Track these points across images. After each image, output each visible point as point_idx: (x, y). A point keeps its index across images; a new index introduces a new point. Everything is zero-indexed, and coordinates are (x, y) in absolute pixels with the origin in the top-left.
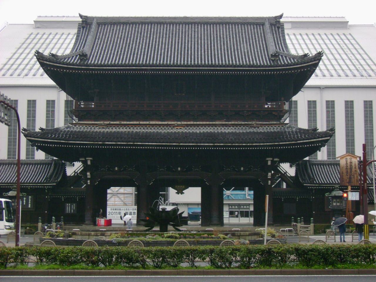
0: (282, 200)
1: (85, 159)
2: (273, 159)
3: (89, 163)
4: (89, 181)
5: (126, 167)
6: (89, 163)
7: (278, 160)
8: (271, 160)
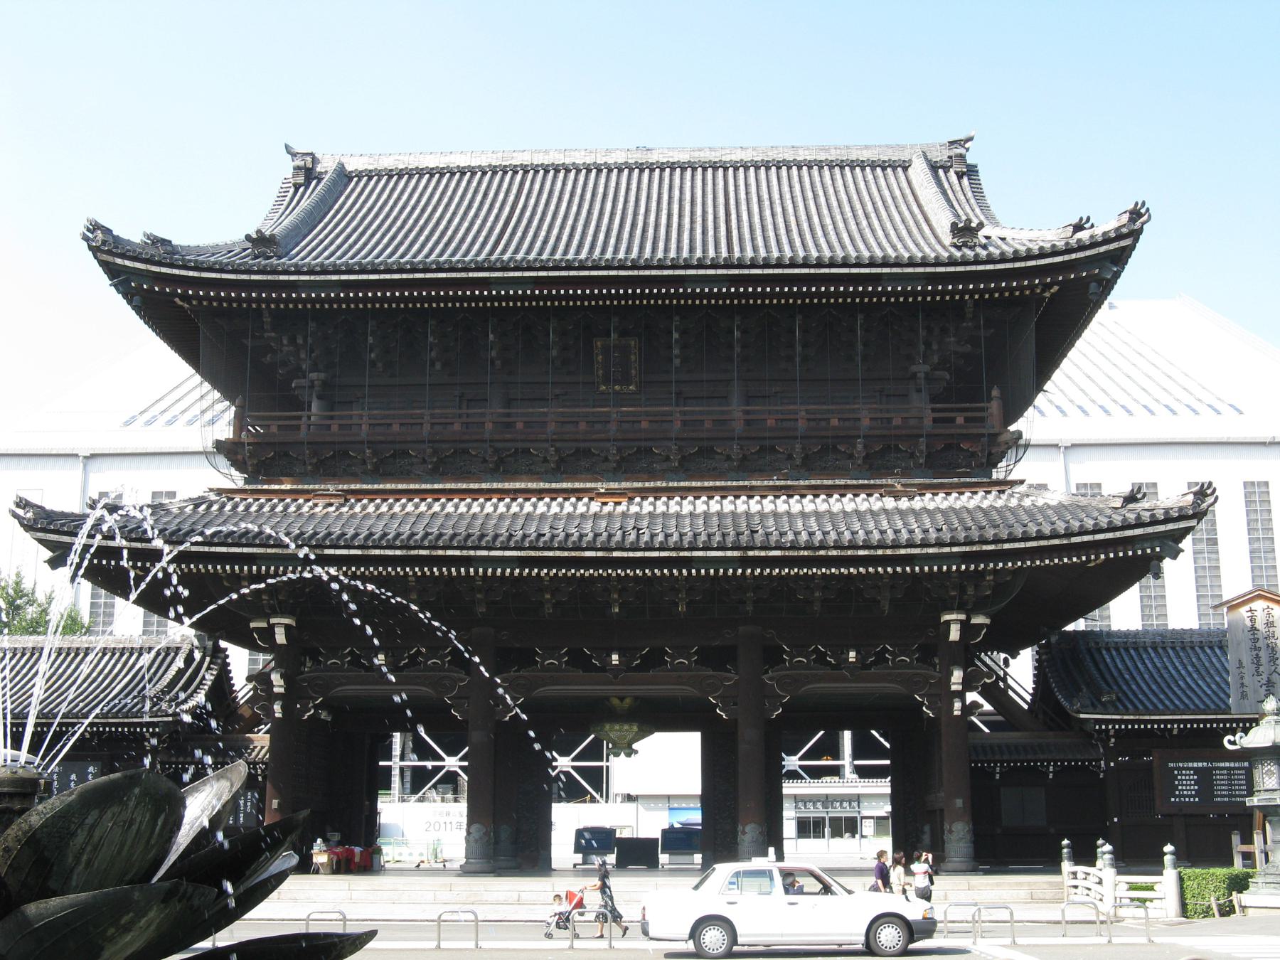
0: (994, 774)
1: (268, 622)
2: (969, 619)
3: (280, 638)
4: (277, 707)
5: (419, 652)
6: (280, 638)
7: (987, 621)
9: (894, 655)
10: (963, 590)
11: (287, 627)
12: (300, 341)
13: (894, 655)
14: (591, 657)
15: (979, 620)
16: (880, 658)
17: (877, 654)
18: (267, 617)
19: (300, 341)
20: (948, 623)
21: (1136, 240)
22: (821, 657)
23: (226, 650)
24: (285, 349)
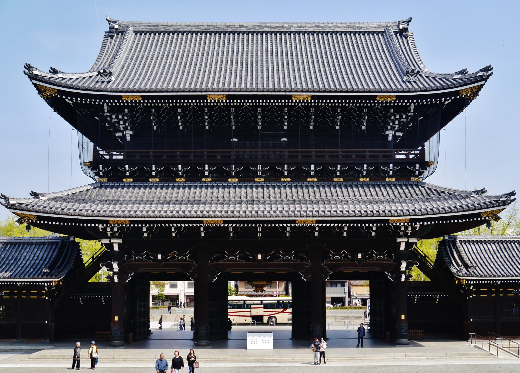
1: (110, 241)
2: (408, 240)
5: (175, 253)
8: (406, 242)
9: (377, 255)
10: (406, 228)
11: (119, 244)
12: (120, 117)
13: (377, 255)
14: (249, 255)
15: (412, 240)
16: (371, 256)
17: (369, 254)
18: (110, 238)
19: (120, 117)
20: (400, 243)
21: (486, 82)
22: (346, 256)
23: (79, 243)
24: (113, 120)
